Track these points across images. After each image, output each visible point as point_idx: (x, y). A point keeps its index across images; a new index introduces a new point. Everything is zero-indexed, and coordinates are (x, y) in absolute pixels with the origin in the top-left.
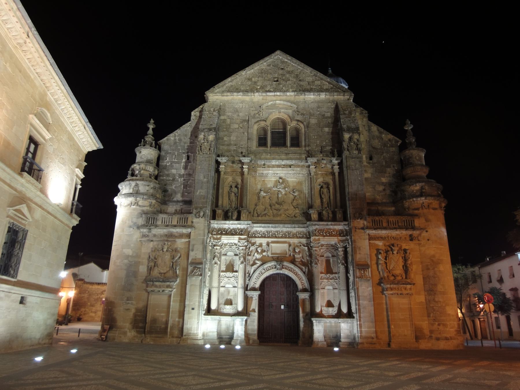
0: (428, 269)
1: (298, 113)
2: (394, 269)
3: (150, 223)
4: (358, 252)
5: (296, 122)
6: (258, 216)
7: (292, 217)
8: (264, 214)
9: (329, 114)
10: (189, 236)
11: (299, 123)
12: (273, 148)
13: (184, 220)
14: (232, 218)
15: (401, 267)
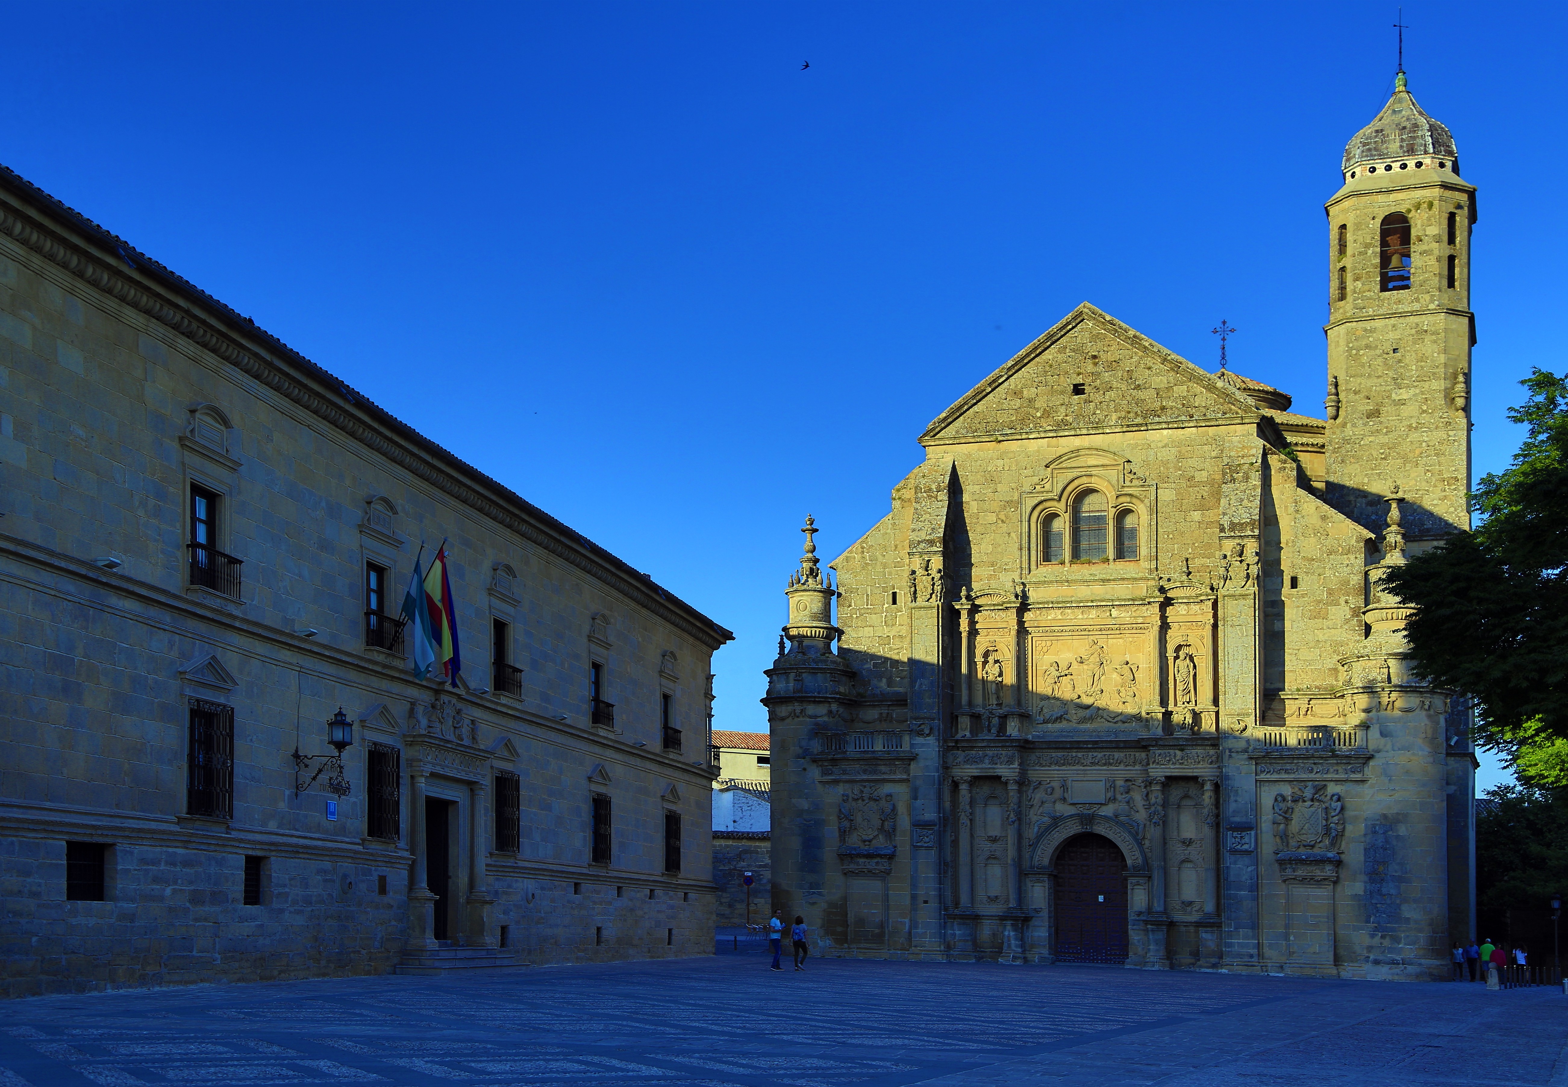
0: (1375, 832)
1: (1132, 476)
2: (1303, 831)
3: (833, 748)
4: (1232, 798)
5: (1128, 499)
6: (1045, 722)
7: (1115, 723)
8: (1057, 719)
9: (1202, 476)
10: (907, 772)
11: (1134, 500)
12: (1074, 566)
13: (894, 740)
14: (989, 731)
15: (1320, 831)
